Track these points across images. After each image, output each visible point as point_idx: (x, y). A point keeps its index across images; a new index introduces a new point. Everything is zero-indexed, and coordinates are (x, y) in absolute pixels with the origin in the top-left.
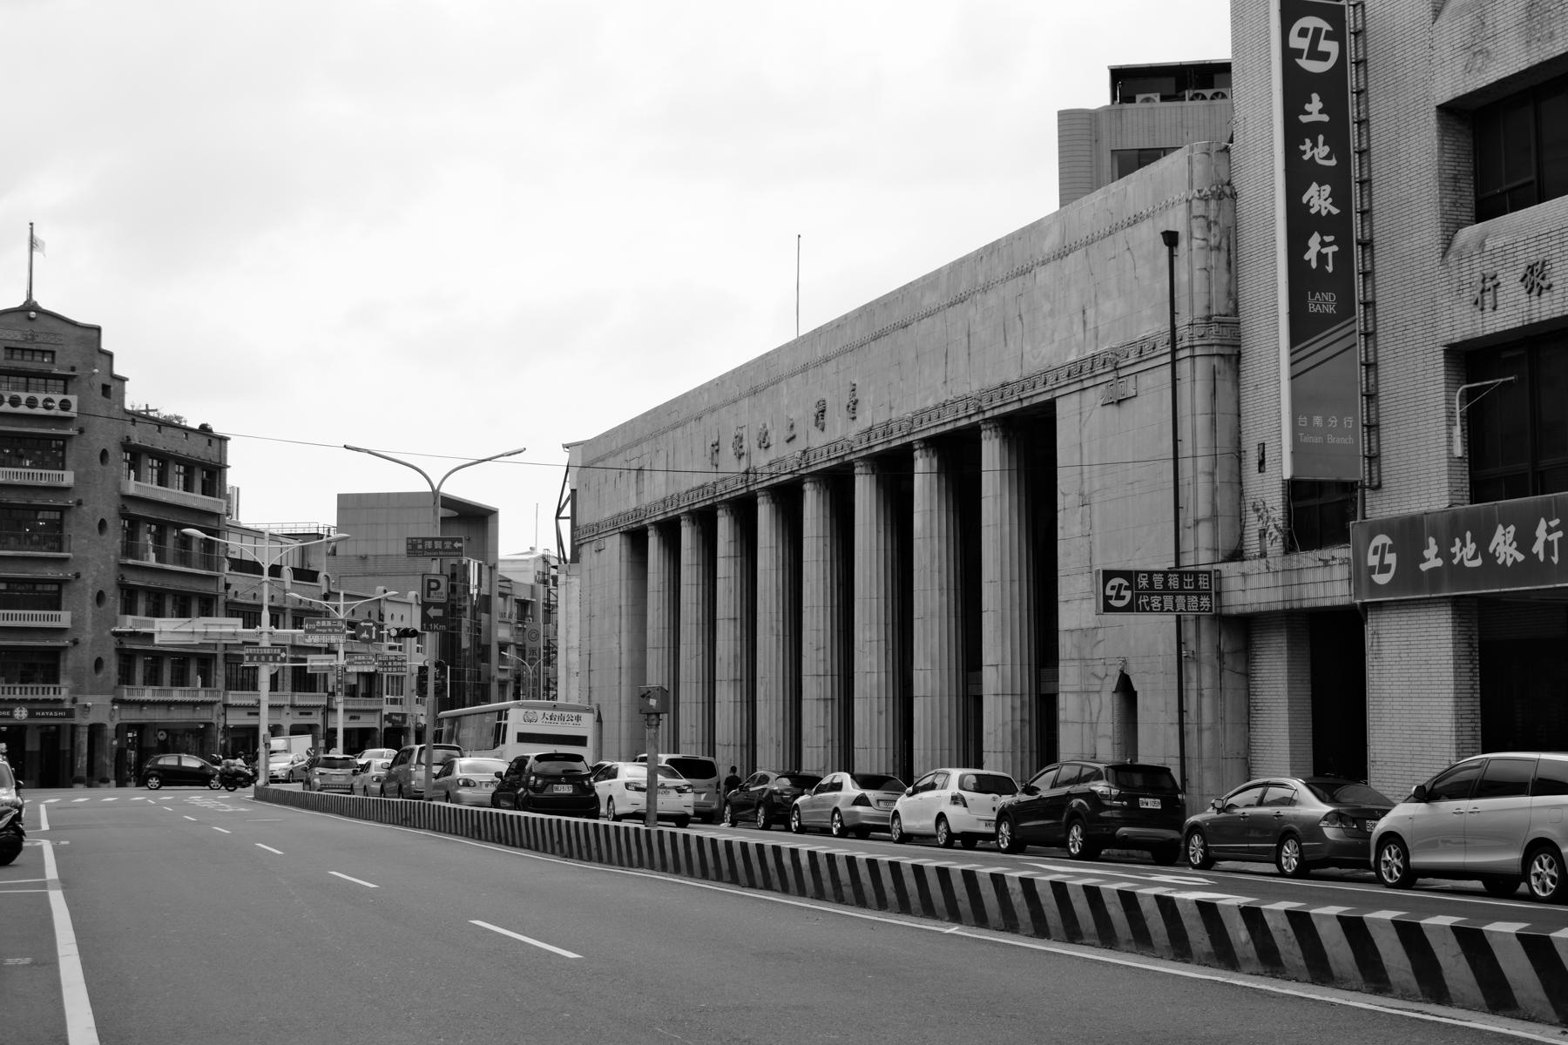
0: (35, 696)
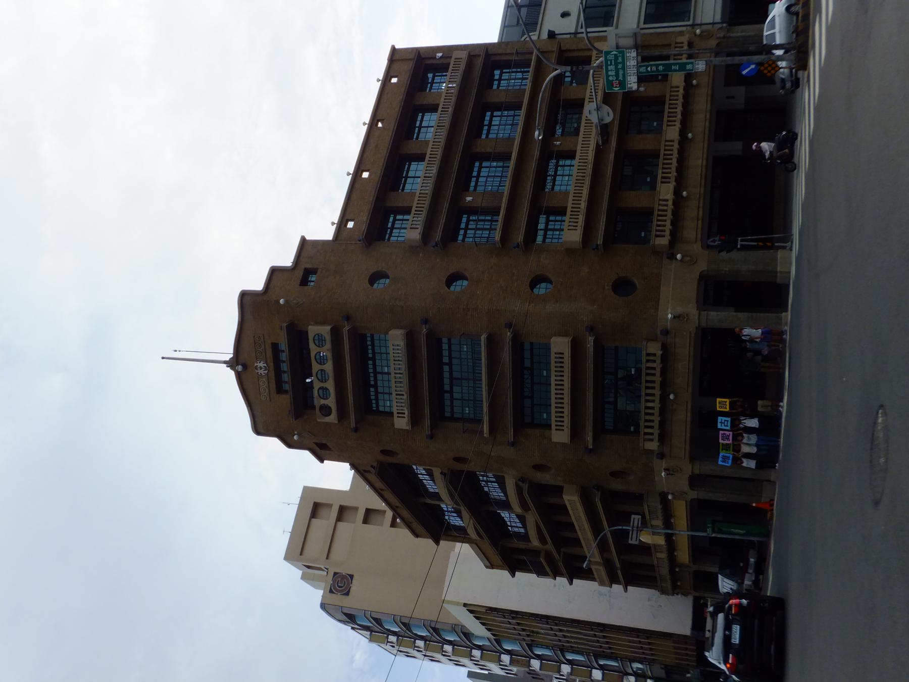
0: (657, 385)
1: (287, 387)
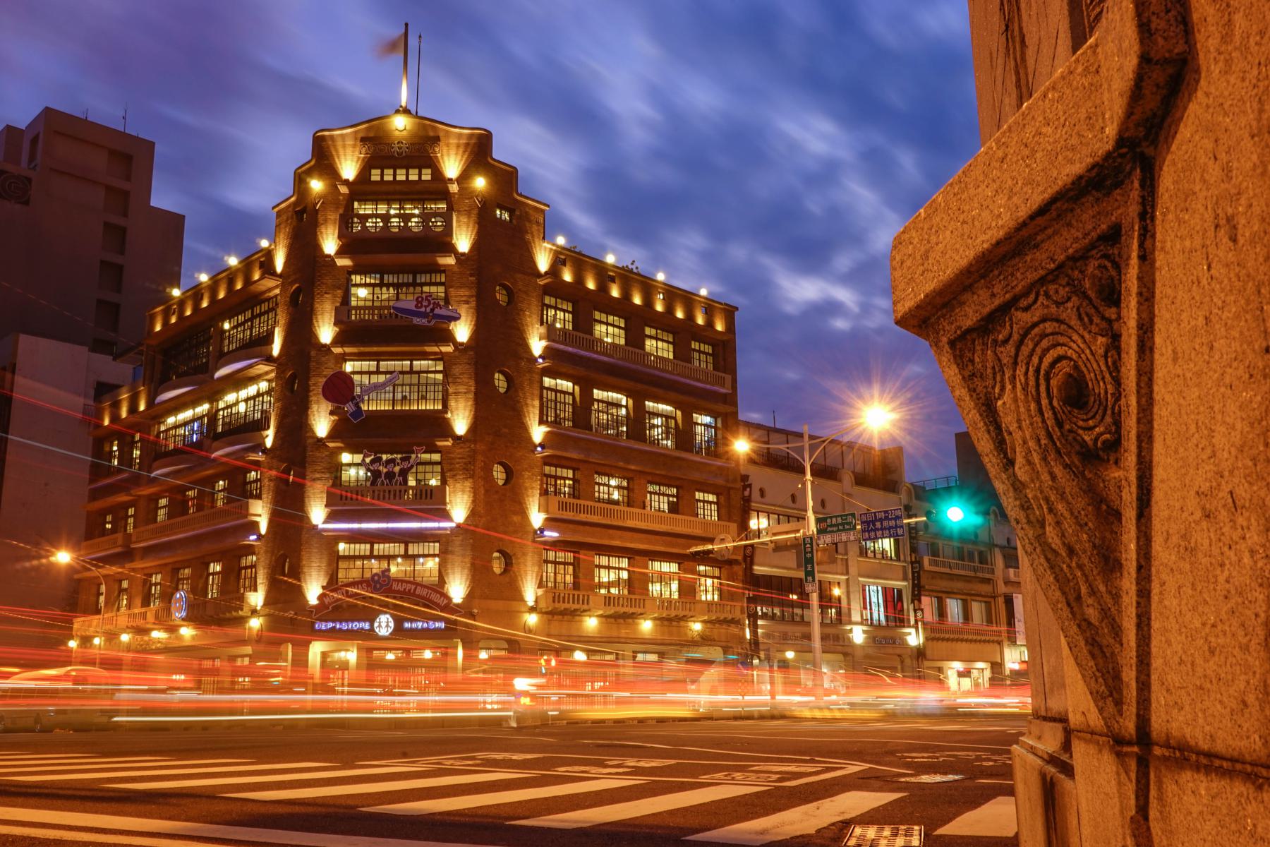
1: (375, 175)
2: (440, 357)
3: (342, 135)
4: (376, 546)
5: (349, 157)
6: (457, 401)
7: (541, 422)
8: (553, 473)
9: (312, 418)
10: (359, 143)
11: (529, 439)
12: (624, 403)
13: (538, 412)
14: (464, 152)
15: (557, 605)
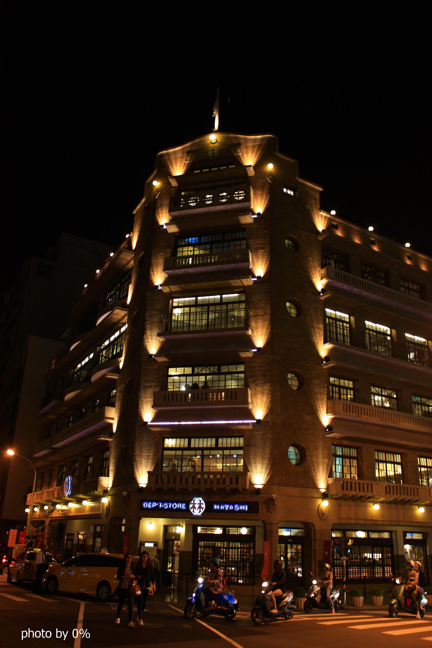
2: (243, 290)
3: (175, 152)
4: (193, 440)
5: (179, 164)
6: (256, 322)
7: (325, 342)
8: (337, 383)
9: (146, 340)
10: (185, 155)
11: (317, 353)
12: (389, 333)
13: (322, 333)
14: (258, 150)
15: (346, 492)
